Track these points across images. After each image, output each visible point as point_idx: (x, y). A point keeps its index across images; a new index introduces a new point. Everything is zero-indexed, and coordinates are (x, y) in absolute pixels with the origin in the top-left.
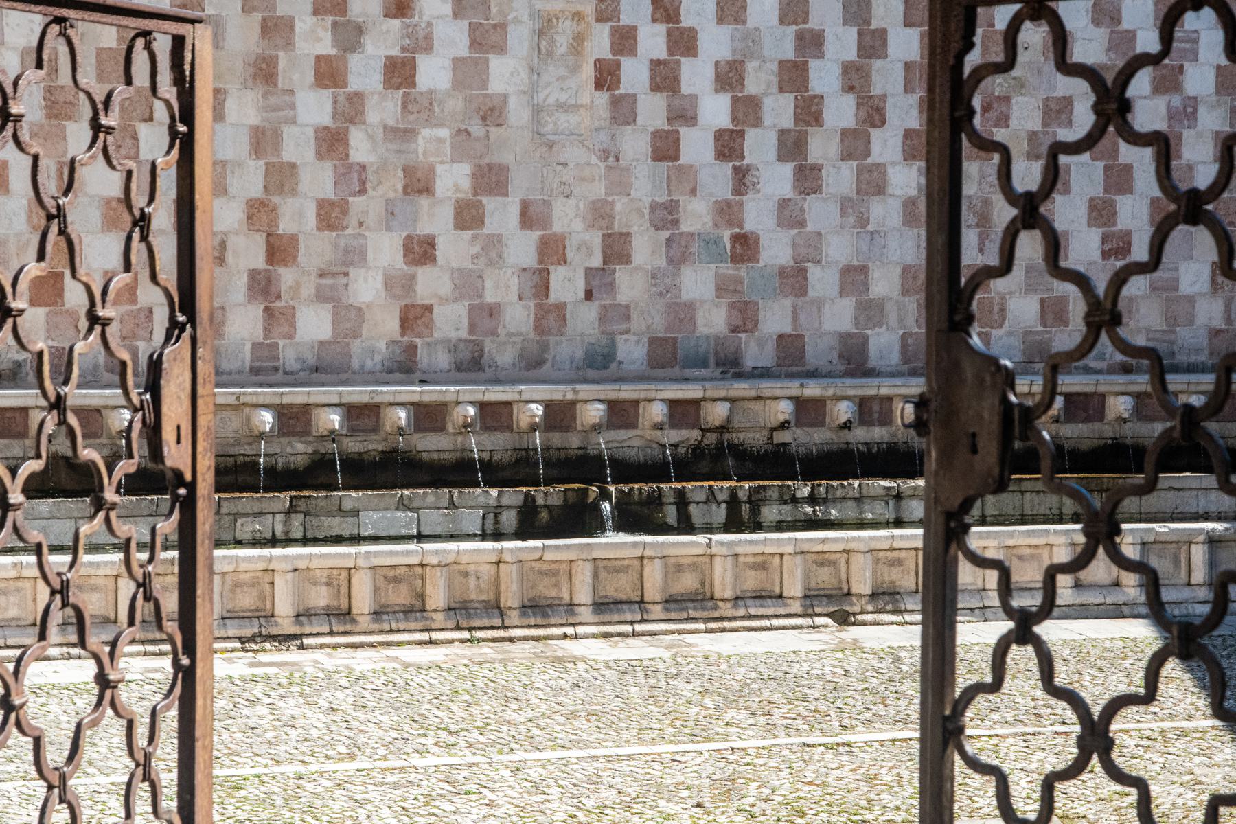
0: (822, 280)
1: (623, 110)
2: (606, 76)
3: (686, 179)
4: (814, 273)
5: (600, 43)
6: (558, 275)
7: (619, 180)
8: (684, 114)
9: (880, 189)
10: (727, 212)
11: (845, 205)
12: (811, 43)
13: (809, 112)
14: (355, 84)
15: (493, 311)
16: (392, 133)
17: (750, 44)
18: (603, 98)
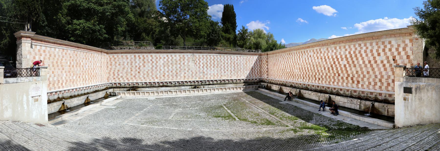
0: (208, 74)
1: (197, 65)
2: (196, 64)
3: (200, 69)
4: (208, 74)
5: (195, 62)
6: (193, 74)
7: (197, 69)
8: (200, 66)
9: (212, 69)
10: (203, 71)
11: (210, 70)
12: (207, 62)
13: (207, 65)
14: (181, 64)
15: (189, 76)
16: (183, 67)
17: (204, 62)
18: (195, 65)
